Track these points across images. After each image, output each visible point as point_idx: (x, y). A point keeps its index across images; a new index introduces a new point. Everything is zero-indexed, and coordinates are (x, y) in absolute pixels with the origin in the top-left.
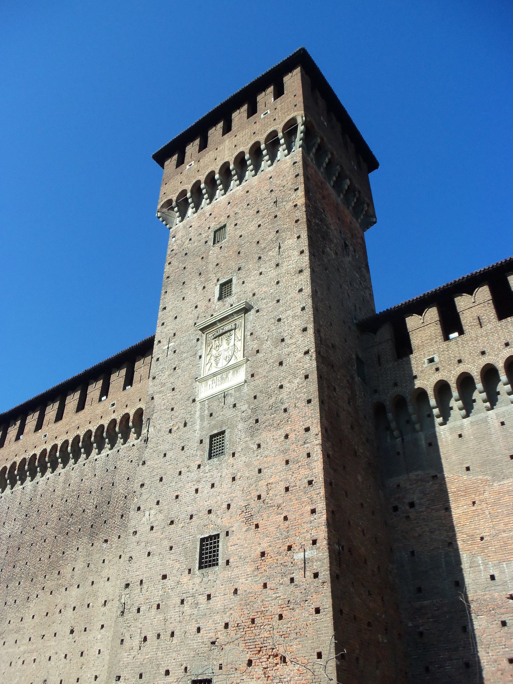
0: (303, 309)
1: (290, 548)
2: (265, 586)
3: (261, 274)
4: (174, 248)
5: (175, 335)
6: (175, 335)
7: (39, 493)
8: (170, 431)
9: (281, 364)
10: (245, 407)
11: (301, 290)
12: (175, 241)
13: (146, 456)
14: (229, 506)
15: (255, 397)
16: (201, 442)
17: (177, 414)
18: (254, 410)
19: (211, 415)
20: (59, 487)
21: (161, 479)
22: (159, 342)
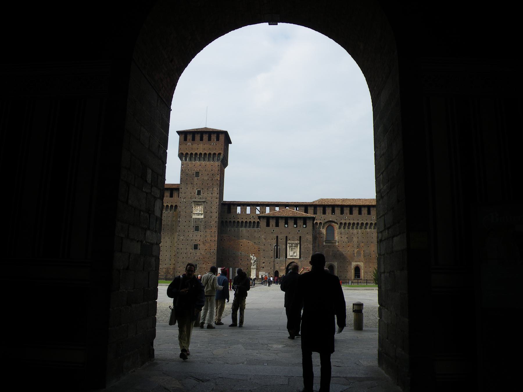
13: (180, 225)
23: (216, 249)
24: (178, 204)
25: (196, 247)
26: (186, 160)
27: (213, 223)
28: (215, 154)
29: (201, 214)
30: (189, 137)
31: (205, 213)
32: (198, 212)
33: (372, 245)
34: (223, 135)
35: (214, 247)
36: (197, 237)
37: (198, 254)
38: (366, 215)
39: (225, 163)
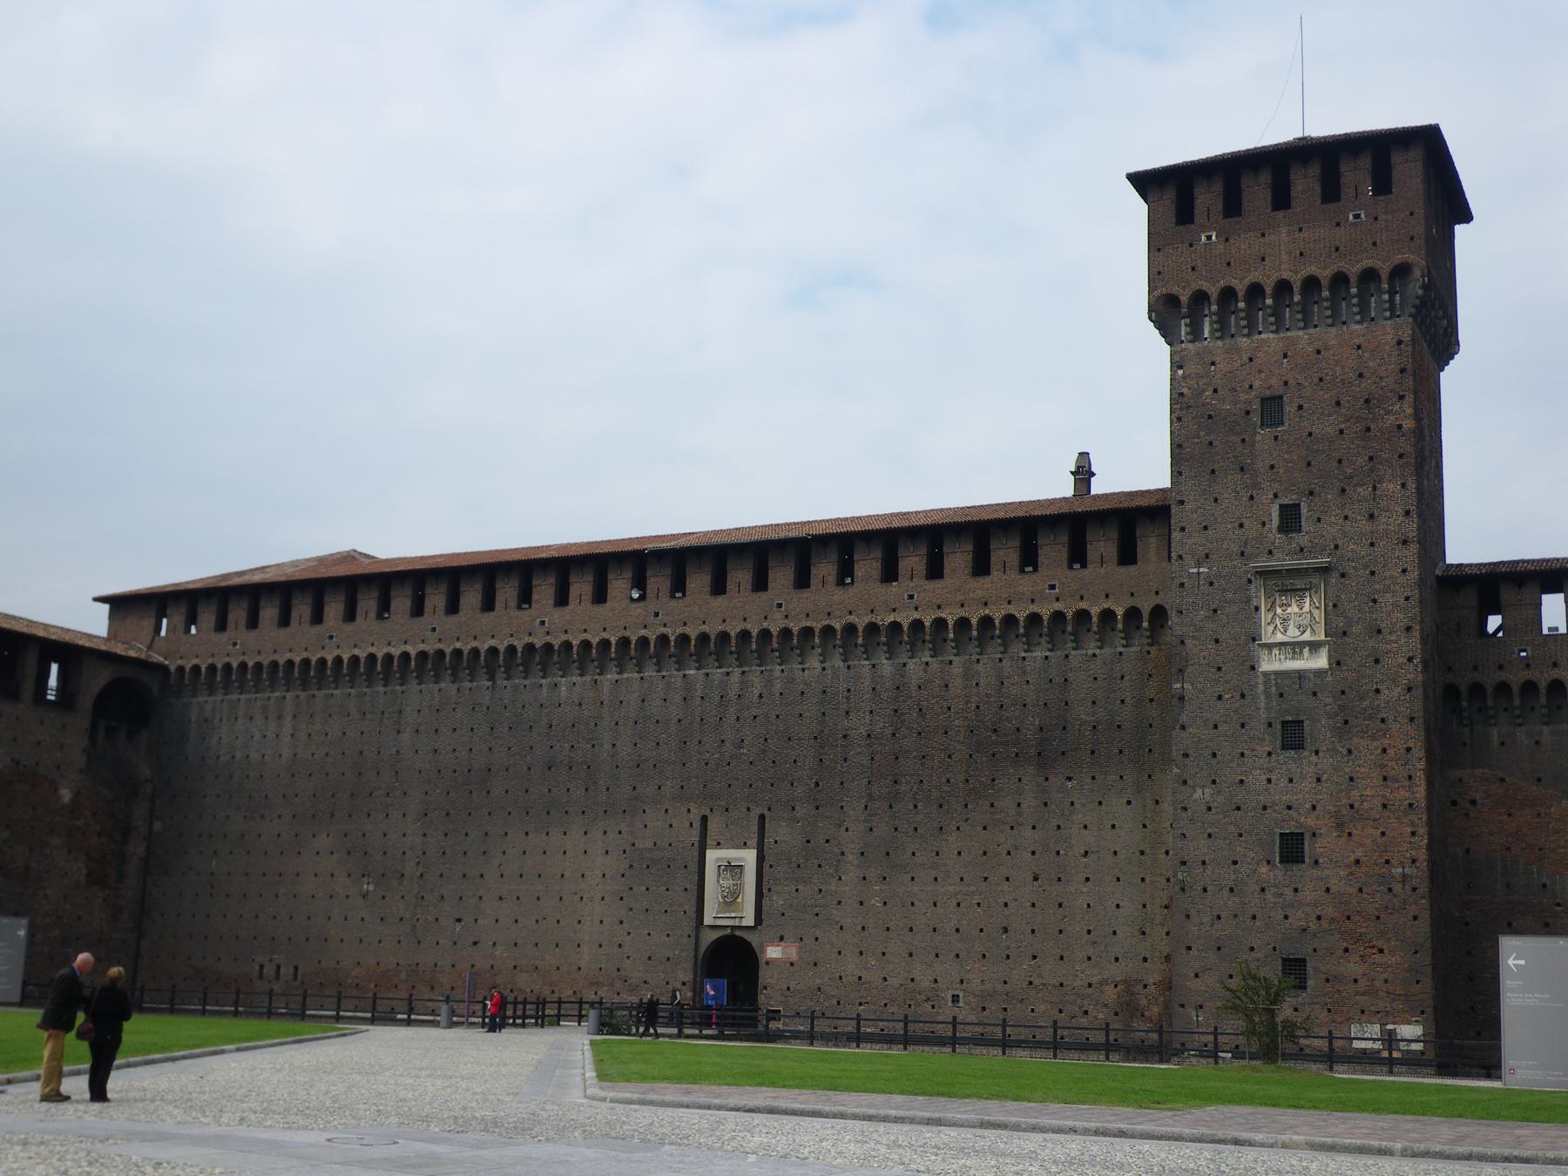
0: (1407, 599)
1: (1387, 862)
2: (1361, 890)
3: (1346, 518)
4: (1185, 391)
5: (1207, 556)
6: (1207, 556)
7: (914, 682)
8: (1220, 697)
9: (1377, 661)
10: (1329, 700)
11: (1404, 571)
12: (1184, 377)
13: (1184, 719)
14: (1314, 807)
15: (1343, 692)
16: (1270, 725)
17: (1228, 677)
18: (1342, 708)
19: (1281, 695)
20: (957, 683)
21: (1214, 755)
22: (1180, 557)
23: (1422, 856)
24: (1170, 600)
25: (1292, 849)
26: (1196, 334)
27: (1392, 693)
28: (1369, 276)
29: (1314, 646)
30: (1207, 198)
32: (1293, 634)
34: (1417, 153)
35: (1410, 845)
36: (1296, 788)
37: (1308, 895)
39: (1437, 335)
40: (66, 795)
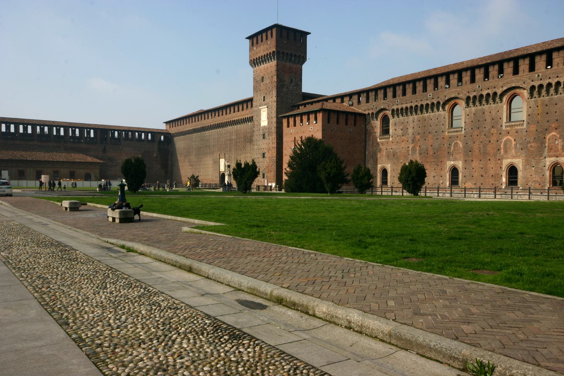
27: (273, 128)
31: (268, 118)
33: (430, 136)
38: (421, 93)
40: (155, 155)
